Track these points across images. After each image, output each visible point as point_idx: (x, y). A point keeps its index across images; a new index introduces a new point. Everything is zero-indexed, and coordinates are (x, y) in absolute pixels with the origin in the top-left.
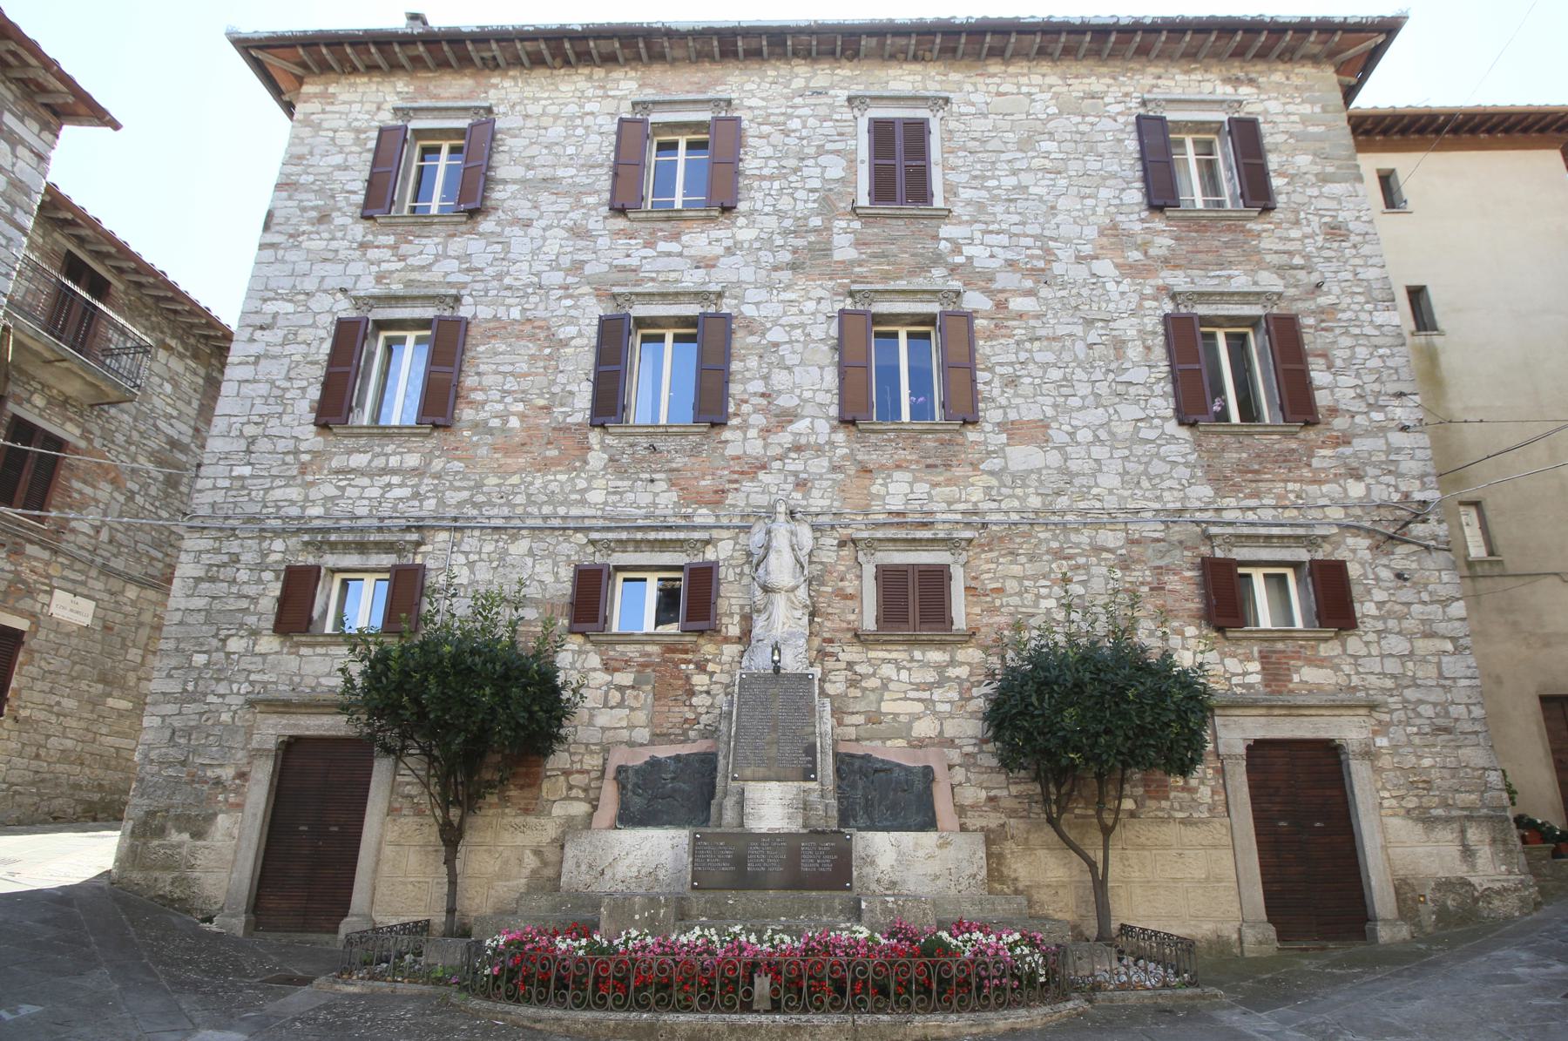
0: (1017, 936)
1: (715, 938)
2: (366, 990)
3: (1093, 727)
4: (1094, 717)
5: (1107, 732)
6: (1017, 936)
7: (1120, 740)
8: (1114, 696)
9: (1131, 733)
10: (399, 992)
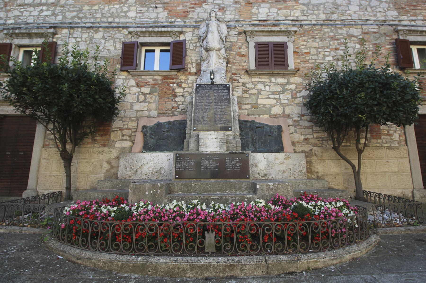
0: (342, 203)
1: (184, 206)
2: (7, 231)
3: (370, 102)
4: (371, 98)
5: (379, 104)
6: (342, 203)
7: (384, 108)
8: (380, 88)
9: (390, 105)
10: (23, 232)
